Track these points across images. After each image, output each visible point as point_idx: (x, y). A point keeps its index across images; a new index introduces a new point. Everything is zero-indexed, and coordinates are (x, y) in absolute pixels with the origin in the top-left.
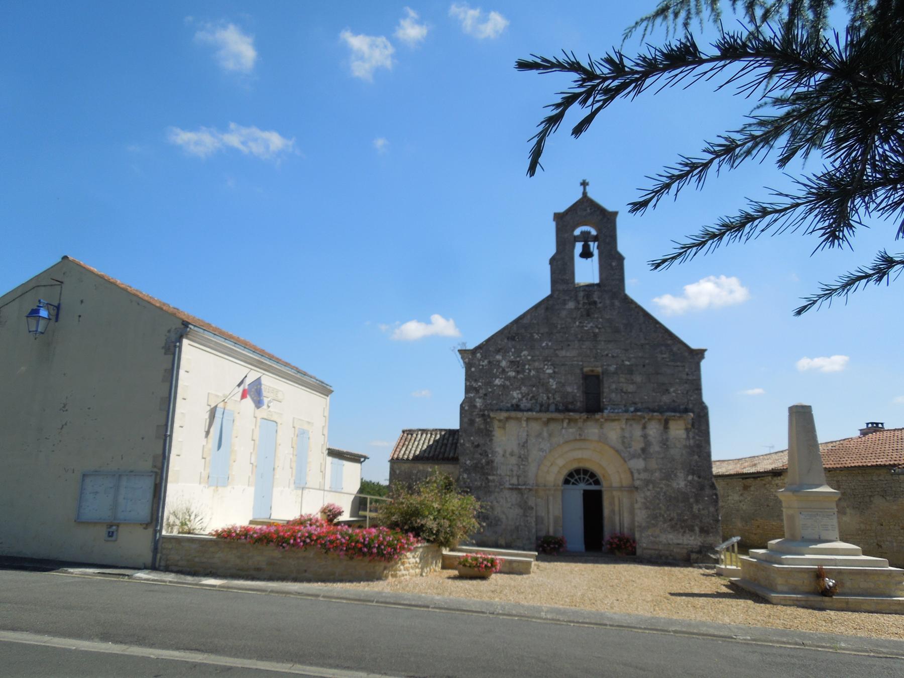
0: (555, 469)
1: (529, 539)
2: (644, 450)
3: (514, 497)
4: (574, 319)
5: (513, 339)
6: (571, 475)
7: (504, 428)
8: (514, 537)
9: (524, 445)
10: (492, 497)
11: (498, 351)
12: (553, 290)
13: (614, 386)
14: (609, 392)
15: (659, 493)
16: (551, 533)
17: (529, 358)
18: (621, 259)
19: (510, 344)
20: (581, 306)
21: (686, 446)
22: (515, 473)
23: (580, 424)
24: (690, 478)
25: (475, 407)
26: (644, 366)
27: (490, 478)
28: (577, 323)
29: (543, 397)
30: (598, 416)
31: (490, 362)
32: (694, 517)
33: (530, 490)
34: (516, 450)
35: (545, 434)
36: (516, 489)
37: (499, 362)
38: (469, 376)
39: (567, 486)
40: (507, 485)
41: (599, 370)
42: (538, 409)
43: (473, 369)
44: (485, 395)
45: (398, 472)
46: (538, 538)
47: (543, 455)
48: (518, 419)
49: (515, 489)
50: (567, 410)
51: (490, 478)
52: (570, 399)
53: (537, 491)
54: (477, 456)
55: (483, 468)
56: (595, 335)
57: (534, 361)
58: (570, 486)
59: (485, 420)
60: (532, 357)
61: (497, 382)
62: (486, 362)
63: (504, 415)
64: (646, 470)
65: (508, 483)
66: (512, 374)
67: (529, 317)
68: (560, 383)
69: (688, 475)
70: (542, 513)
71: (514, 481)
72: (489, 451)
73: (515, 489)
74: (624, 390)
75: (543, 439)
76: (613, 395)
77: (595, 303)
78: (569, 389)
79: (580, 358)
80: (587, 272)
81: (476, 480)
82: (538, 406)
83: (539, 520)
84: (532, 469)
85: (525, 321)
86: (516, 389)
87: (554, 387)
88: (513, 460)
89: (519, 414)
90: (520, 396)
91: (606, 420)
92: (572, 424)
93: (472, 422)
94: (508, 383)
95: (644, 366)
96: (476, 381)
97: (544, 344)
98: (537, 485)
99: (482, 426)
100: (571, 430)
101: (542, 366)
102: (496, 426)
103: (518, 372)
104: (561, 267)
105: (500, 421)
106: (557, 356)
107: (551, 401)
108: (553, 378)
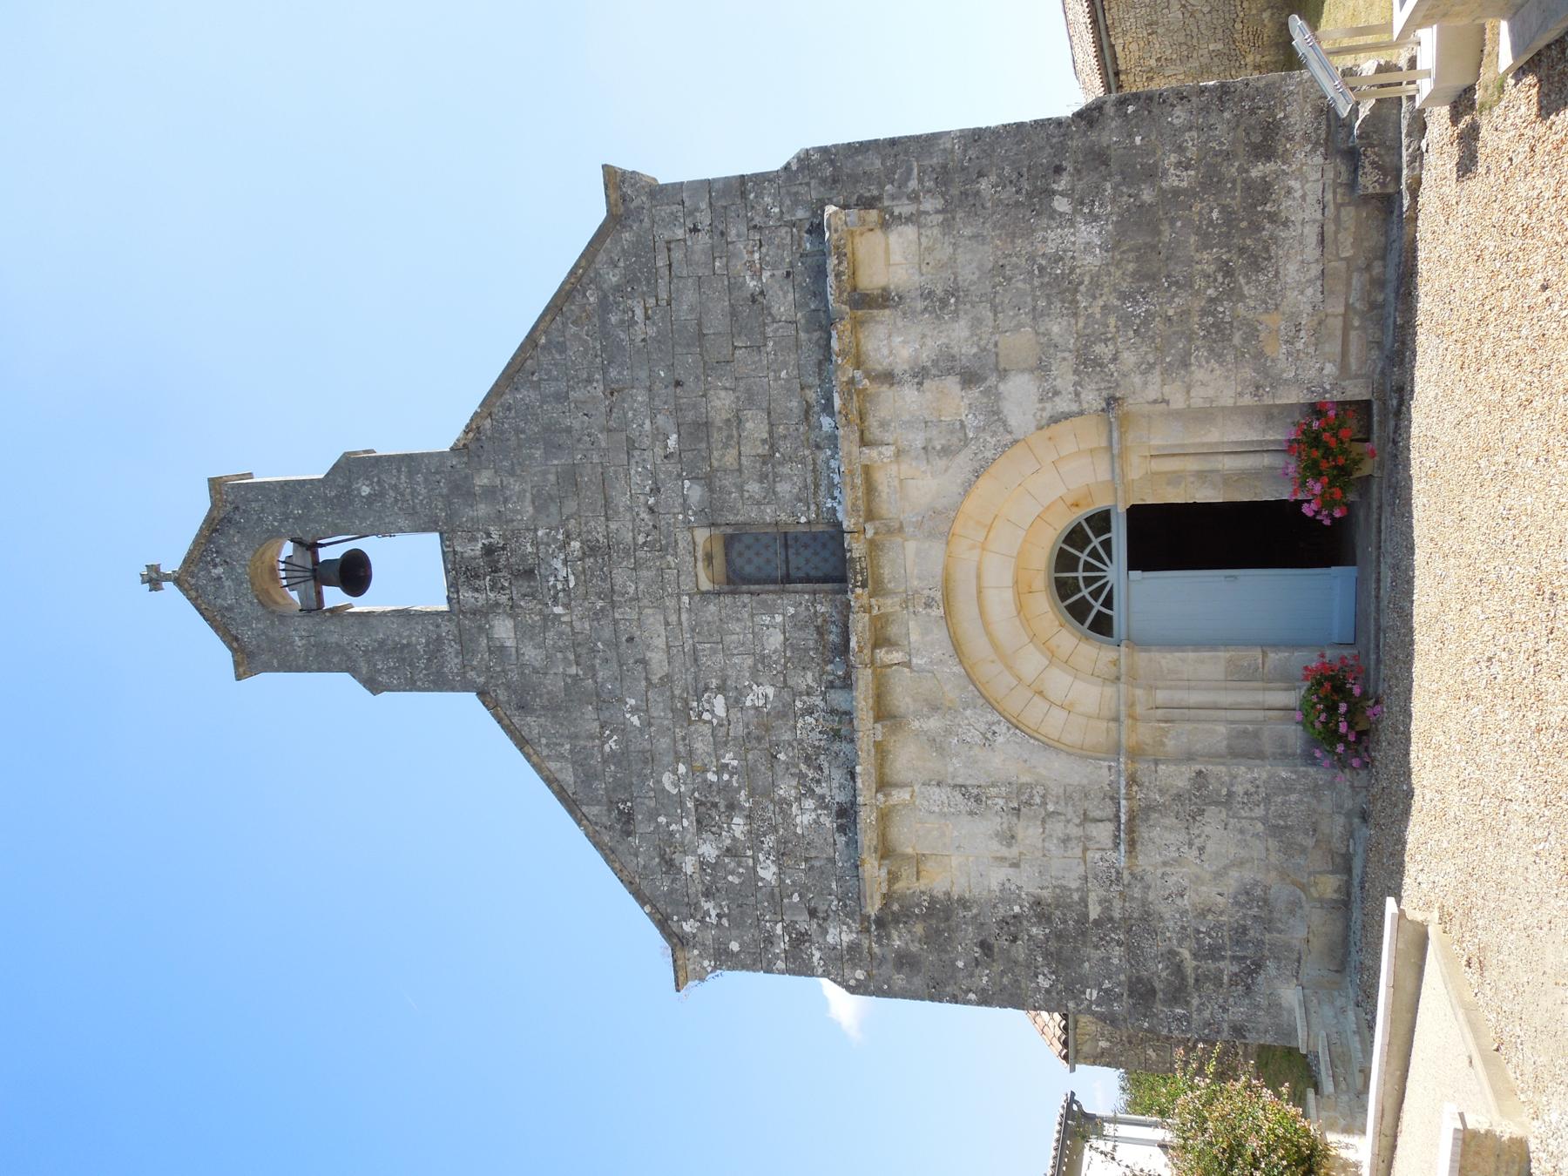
0: (1059, 682)
1: (1315, 790)
2: (970, 378)
3: (1162, 838)
4: (549, 620)
5: (627, 818)
6: (1078, 611)
7: (919, 861)
8: (1309, 842)
9: (975, 797)
10: (1166, 910)
11: (670, 866)
12: (466, 687)
13: (753, 488)
14: (777, 504)
15: (1125, 320)
16: (1290, 698)
17: (682, 769)
18: (352, 467)
19: (644, 827)
20: (503, 599)
21: (947, 226)
22: (1074, 831)
23: (890, 605)
24: (1061, 205)
25: (853, 948)
26: (678, 384)
27: (1094, 912)
28: (558, 610)
29: (809, 729)
30: (856, 548)
31: (708, 894)
32: (1211, 182)
33: (1133, 780)
34: (994, 823)
35: (934, 724)
36: (1131, 831)
37: (703, 864)
38: (757, 959)
39: (1119, 625)
40: (1120, 858)
41: (702, 535)
42: (845, 747)
43: (735, 946)
44: (813, 913)
45: (1103, 1044)
46: (1310, 759)
47: (1016, 716)
48: (884, 816)
49: (1129, 835)
50: (843, 648)
51: (1094, 912)
52: (810, 638)
53: (1135, 754)
54: (1020, 951)
55: (1059, 936)
56: (591, 550)
57: (691, 752)
58: (1118, 614)
59: (896, 920)
60: (678, 758)
61: (768, 873)
62: (708, 905)
63: (873, 870)
64: (1041, 368)
65: (1112, 856)
66: (739, 825)
67: (553, 765)
68: (754, 672)
69: (1053, 214)
70: (1218, 734)
71: (1103, 833)
72: (1002, 911)
73: (1129, 835)
74: (764, 450)
75: (948, 731)
76: (783, 488)
77: (489, 550)
78: (775, 640)
79: (670, 603)
80: (409, 572)
81: (1106, 960)
82: (836, 747)
83: (1243, 749)
84: (1058, 771)
85: (568, 777)
86: (786, 815)
87: (770, 691)
88: (1030, 833)
89: (867, 817)
90: (809, 803)
91: (870, 516)
92: (893, 631)
93: (904, 961)
94: (769, 841)
95: (678, 384)
96: (770, 940)
97: (635, 720)
98: (1116, 750)
99: (919, 929)
100: (914, 637)
101: (706, 729)
102: (922, 885)
103: (732, 807)
104: (398, 659)
105: (893, 878)
106: (667, 679)
107: (818, 701)
108: (741, 693)
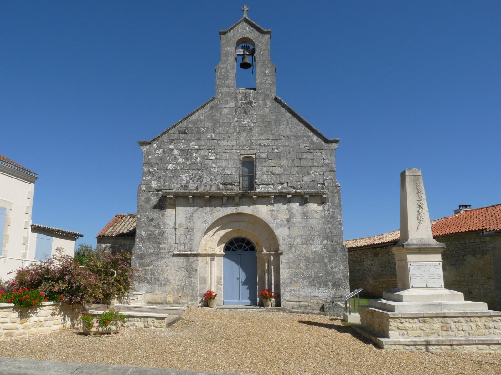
2: (288, 221)
5: (184, 132)
11: (171, 142)
13: (265, 169)
15: (299, 255)
17: (196, 147)
21: (322, 217)
24: (325, 242)
25: (151, 187)
26: (289, 153)
27: (162, 246)
28: (236, 119)
31: (164, 151)
32: (328, 273)
37: (172, 150)
43: (150, 157)
51: (162, 246)
54: (151, 228)
61: (170, 167)
64: (289, 236)
66: (182, 160)
69: (323, 240)
72: (161, 224)
76: (265, 176)
77: (251, 102)
78: (229, 172)
79: (238, 147)
81: (150, 248)
90: (188, 178)
92: (230, 201)
94: (178, 168)
95: (289, 153)
96: (152, 166)
97: (209, 136)
103: (187, 159)
106: (219, 145)
107: (214, 182)
108: (216, 163)
